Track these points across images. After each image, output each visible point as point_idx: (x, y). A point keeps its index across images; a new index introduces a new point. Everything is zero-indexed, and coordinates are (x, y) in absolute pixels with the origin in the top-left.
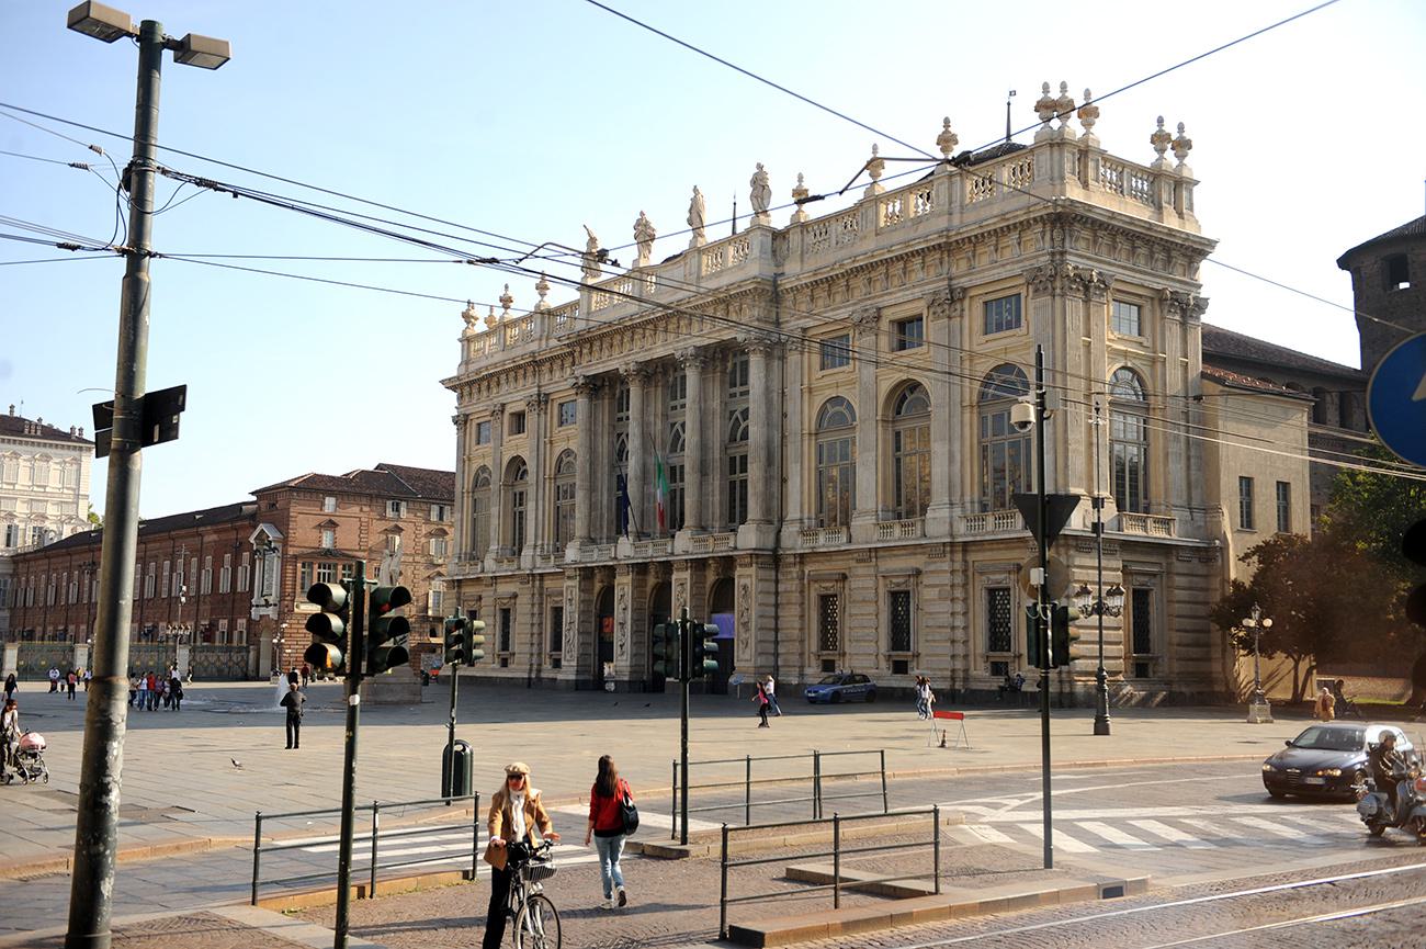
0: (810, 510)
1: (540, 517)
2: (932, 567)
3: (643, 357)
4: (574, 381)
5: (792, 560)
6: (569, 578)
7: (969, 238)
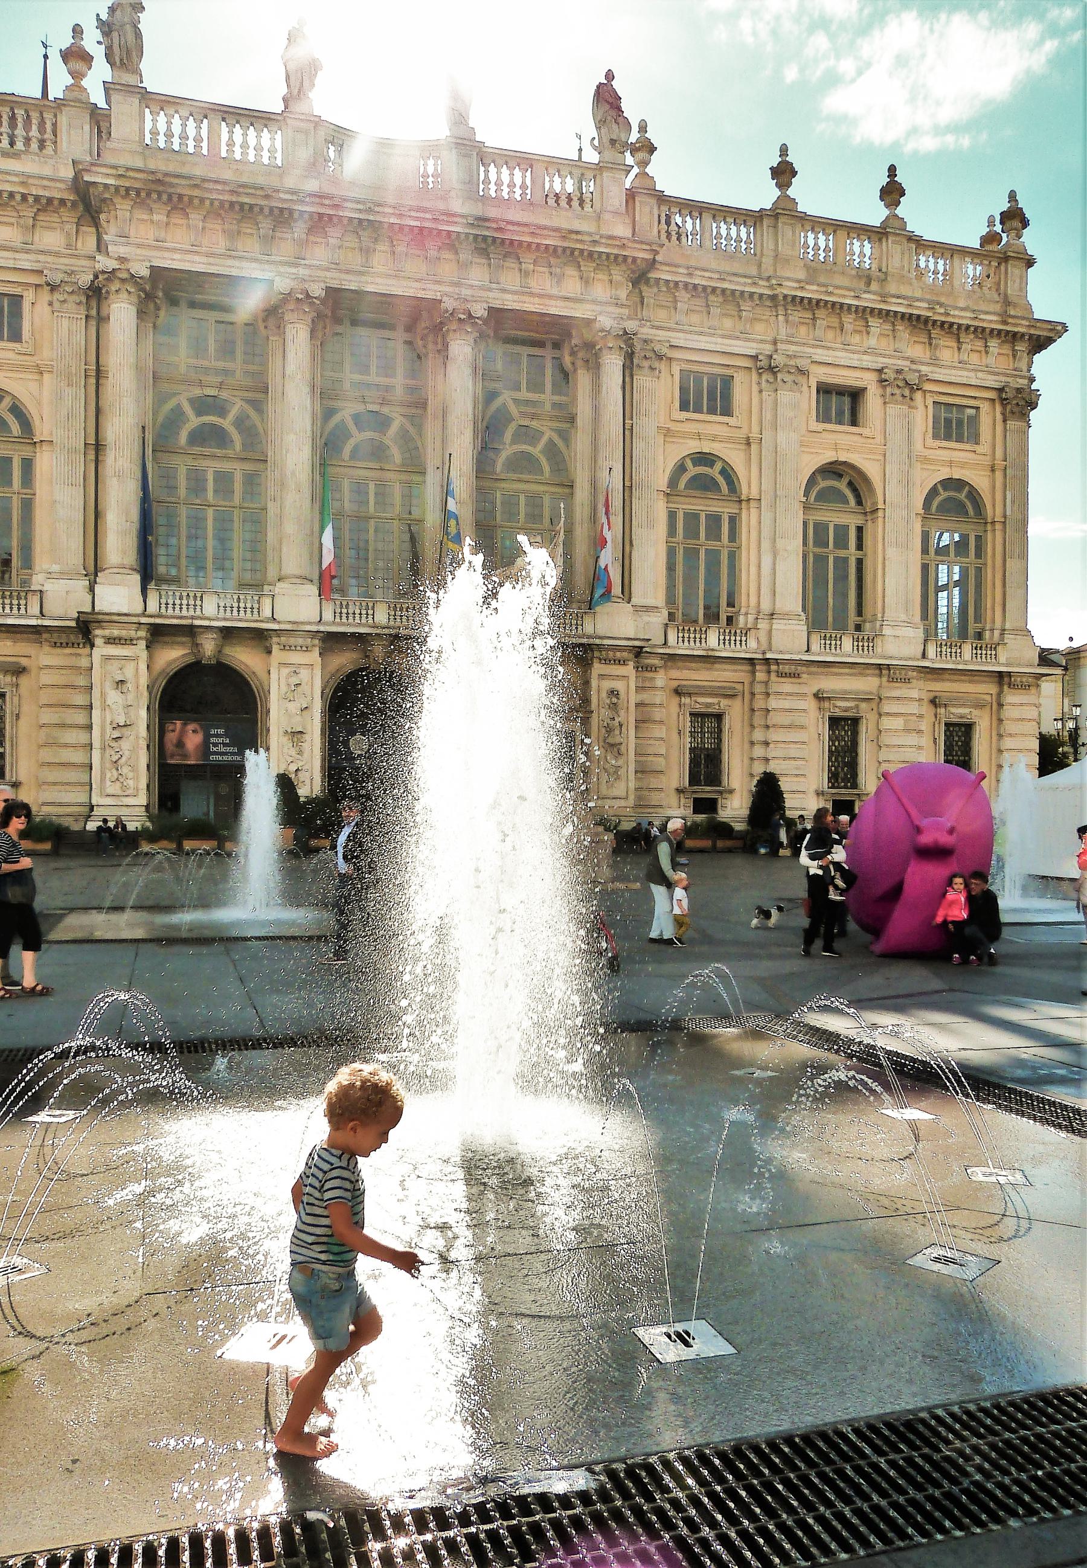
0: (659, 599)
3: (336, 280)
4: (114, 264)
5: (656, 662)
6: (110, 641)
7: (952, 324)
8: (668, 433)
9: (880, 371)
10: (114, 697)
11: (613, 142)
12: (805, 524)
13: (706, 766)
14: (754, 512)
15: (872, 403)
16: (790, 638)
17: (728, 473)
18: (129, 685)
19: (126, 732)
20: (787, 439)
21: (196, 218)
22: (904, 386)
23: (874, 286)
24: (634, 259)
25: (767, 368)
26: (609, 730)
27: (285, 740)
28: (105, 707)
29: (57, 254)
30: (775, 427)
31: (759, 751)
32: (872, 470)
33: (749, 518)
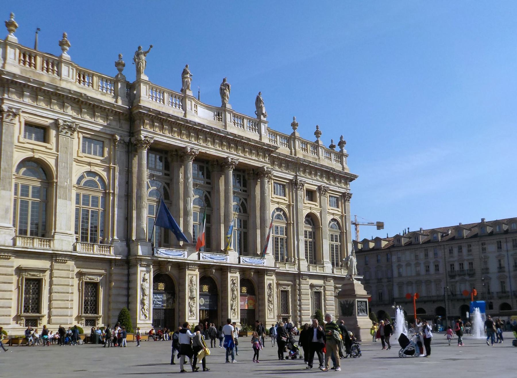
6: (141, 266)
8: (273, 201)
16: (304, 266)
18: (148, 281)
32: (318, 215)
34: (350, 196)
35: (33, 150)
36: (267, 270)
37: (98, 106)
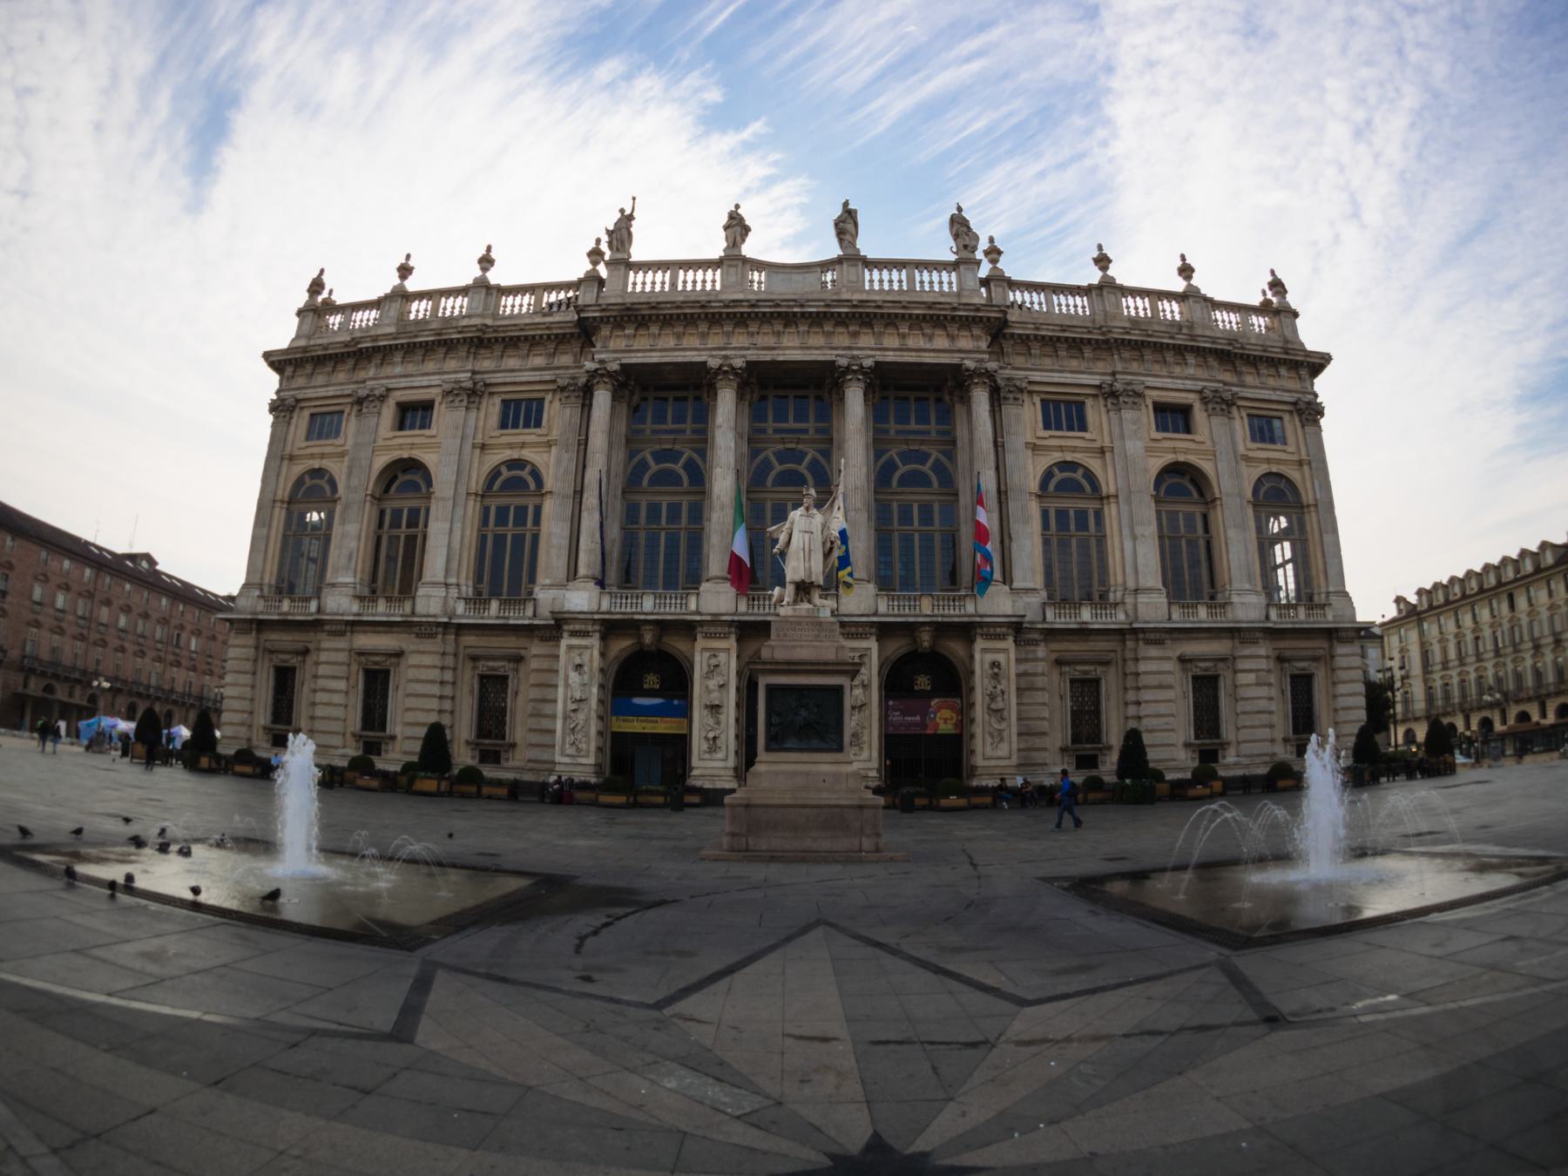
0: (1038, 582)
1: (456, 545)
2: (1247, 652)
3: (753, 355)
5: (1036, 636)
6: (574, 634)
8: (1034, 448)
9: (1200, 392)
10: (574, 677)
11: (966, 247)
12: (1158, 513)
13: (1086, 723)
14: (1113, 506)
15: (1199, 415)
16: (1154, 608)
17: (1090, 475)
19: (582, 705)
20: (1134, 446)
21: (654, 329)
22: (1222, 404)
23: (1185, 331)
24: (989, 318)
25: (1110, 395)
26: (993, 698)
27: (705, 712)
28: (567, 685)
29: (567, 368)
30: (1122, 437)
31: (1132, 710)
32: (1207, 467)
33: (1111, 511)
34: (1319, 411)
35: (400, 447)
36: (981, 625)
37: (518, 338)
